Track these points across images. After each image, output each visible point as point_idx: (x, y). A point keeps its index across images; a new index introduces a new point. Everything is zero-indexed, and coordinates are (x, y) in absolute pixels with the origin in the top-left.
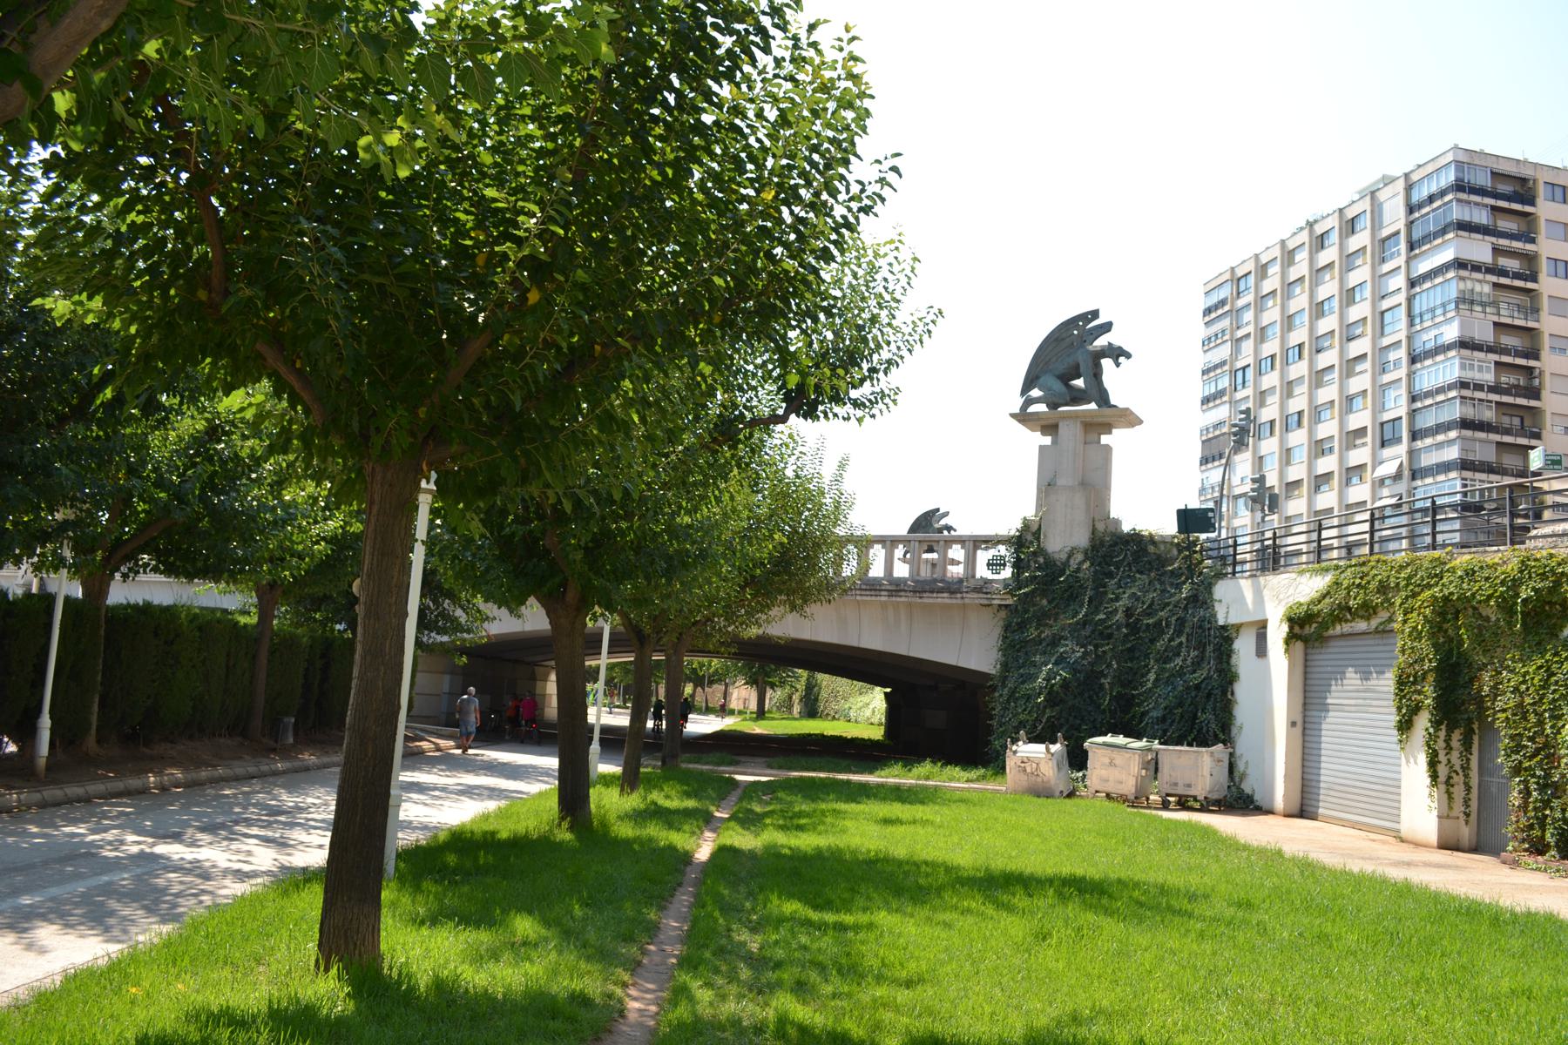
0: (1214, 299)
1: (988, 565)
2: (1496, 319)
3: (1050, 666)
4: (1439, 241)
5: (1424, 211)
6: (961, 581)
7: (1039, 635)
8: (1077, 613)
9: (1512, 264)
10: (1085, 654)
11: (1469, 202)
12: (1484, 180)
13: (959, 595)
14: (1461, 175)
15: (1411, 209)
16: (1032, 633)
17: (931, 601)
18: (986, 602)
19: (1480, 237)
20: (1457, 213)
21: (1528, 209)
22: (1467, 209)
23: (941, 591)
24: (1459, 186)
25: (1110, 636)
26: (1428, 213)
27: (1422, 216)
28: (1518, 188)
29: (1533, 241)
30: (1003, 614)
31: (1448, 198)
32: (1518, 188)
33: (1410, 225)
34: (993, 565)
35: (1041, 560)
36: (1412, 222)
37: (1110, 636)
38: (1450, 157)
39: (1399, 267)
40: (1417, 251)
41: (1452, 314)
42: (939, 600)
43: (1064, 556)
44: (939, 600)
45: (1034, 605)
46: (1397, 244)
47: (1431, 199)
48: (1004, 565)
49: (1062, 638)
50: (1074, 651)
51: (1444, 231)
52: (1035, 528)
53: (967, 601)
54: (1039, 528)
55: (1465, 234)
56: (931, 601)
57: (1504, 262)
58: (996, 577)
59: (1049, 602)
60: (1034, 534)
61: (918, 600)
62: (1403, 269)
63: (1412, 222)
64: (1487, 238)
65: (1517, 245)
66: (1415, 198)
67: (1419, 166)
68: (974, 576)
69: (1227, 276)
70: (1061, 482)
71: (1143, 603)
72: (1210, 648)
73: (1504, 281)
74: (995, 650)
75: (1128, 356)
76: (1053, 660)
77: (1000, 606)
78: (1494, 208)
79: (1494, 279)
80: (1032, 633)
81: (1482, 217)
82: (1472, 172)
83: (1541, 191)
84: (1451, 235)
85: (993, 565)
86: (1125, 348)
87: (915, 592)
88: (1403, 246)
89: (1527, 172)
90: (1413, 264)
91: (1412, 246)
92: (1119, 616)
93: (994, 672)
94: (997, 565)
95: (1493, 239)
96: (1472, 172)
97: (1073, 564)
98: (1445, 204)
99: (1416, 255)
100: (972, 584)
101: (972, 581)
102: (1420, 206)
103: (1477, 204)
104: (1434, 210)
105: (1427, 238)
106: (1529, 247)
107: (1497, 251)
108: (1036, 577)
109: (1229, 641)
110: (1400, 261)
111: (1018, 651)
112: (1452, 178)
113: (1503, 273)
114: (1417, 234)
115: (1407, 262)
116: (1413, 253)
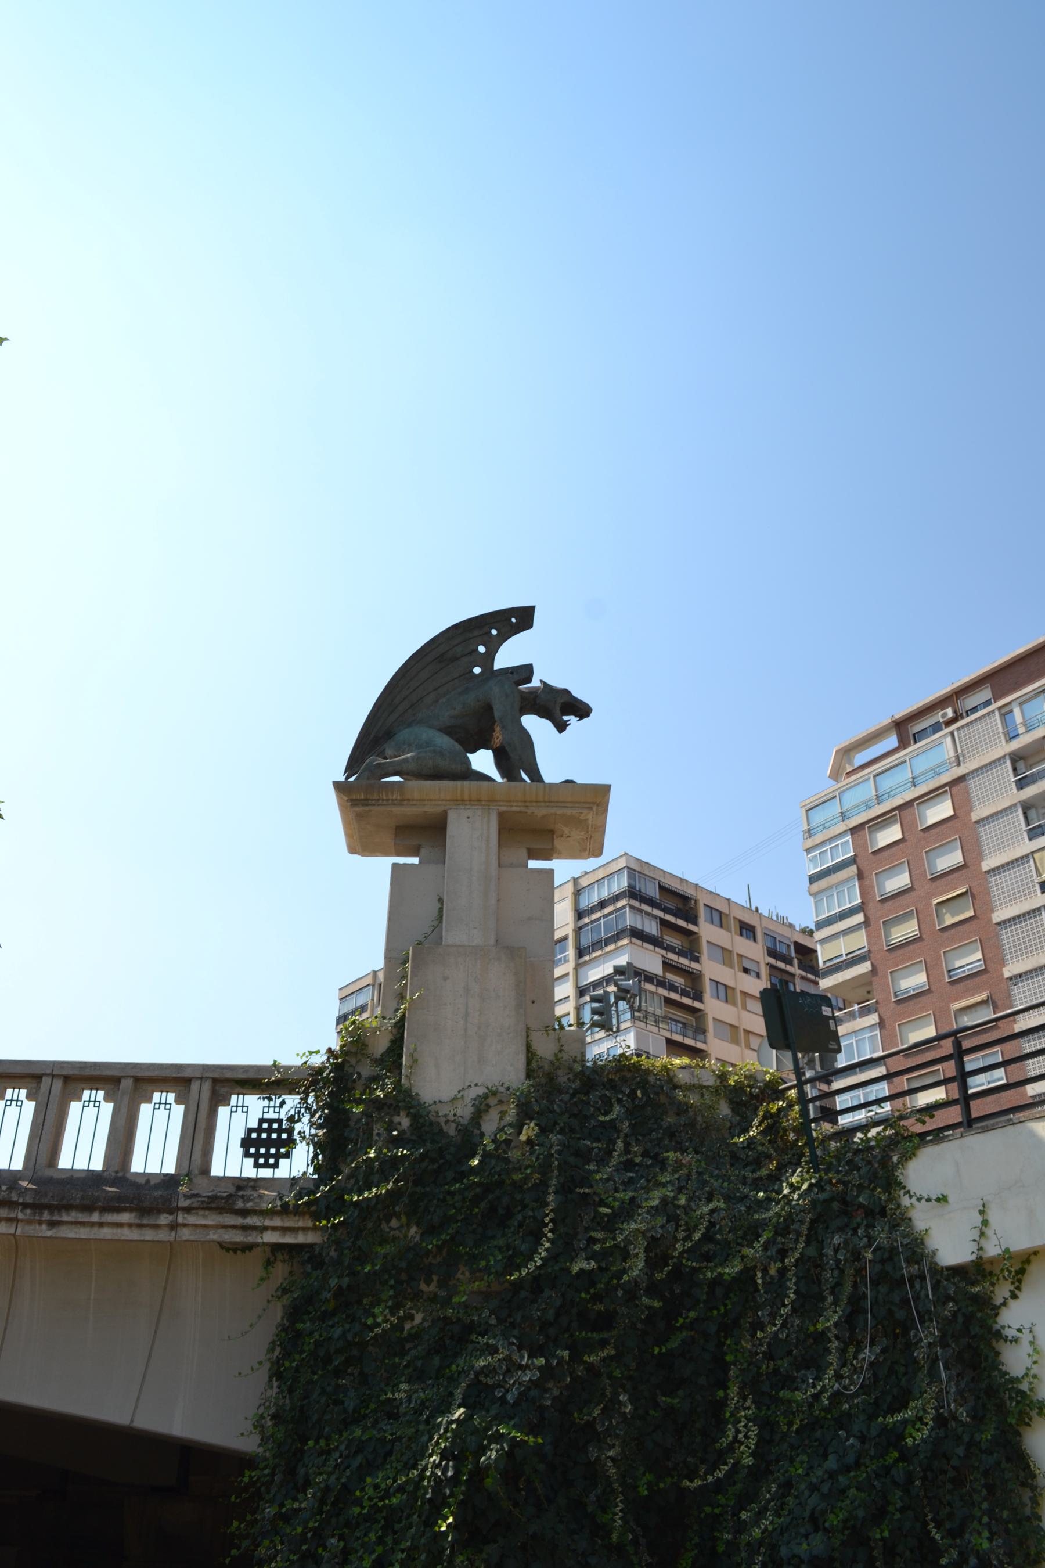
0: (351, 1005)
1: (246, 1143)
2: (668, 1035)
3: (459, 1413)
4: (612, 947)
5: (594, 916)
6: (169, 1181)
7: (398, 1327)
8: (512, 1265)
9: (678, 981)
10: (547, 1371)
11: (641, 911)
12: (653, 892)
13: (164, 1219)
14: (633, 883)
15: (579, 914)
16: (382, 1319)
17: (83, 1233)
18: (238, 1237)
19: (651, 947)
20: (630, 920)
21: (692, 927)
22: (639, 918)
23: (113, 1206)
24: (632, 893)
25: (606, 1321)
26: (599, 919)
27: (592, 922)
28: (680, 906)
29: (697, 960)
30: (280, 1271)
31: (619, 904)
32: (680, 906)
33: (578, 930)
34: (258, 1143)
35: (405, 1122)
36: (580, 928)
37: (606, 1321)
38: (622, 863)
39: (567, 974)
40: (587, 958)
41: (628, 1024)
42: (106, 1233)
43: (465, 1112)
44: (106, 1233)
45: (383, 1241)
46: (564, 950)
47: (602, 904)
48: (291, 1143)
49: (470, 1328)
50: (512, 1367)
51: (617, 937)
52: (381, 1045)
53: (185, 1234)
54: (397, 1043)
55: (639, 942)
56: (83, 1233)
57: (670, 976)
58: (265, 1173)
59: (430, 1231)
60: (380, 1062)
61: (45, 1231)
62: (571, 976)
63: (580, 928)
64: (657, 949)
65: (684, 961)
66: (585, 903)
67: (586, 873)
68: (206, 1170)
69: (369, 980)
70: (453, 936)
71: (690, 1230)
72: (927, 1334)
73: (674, 996)
74: (264, 1373)
75: (582, 711)
76: (458, 1394)
77: (276, 1247)
78: (663, 923)
79: (664, 992)
80: (382, 1319)
81: (652, 928)
82: (642, 881)
83: (702, 912)
84: (625, 941)
85: (258, 1143)
86: (579, 693)
87: (37, 1207)
88: (571, 952)
89: (690, 892)
90: (582, 971)
91: (580, 953)
92: (637, 1267)
93: (250, 1445)
94: (268, 1143)
95: (663, 952)
96: (642, 881)
97: (490, 1125)
98: (617, 910)
99: (586, 962)
100: (203, 1188)
101: (200, 1183)
102: (592, 910)
103: (647, 914)
104: (605, 916)
105: (596, 945)
106: (694, 965)
107: (667, 965)
108: (395, 1162)
109: (986, 1307)
110: (569, 967)
111: (338, 1373)
112: (624, 883)
113: (672, 988)
114: (586, 940)
115: (576, 969)
116: (582, 960)
